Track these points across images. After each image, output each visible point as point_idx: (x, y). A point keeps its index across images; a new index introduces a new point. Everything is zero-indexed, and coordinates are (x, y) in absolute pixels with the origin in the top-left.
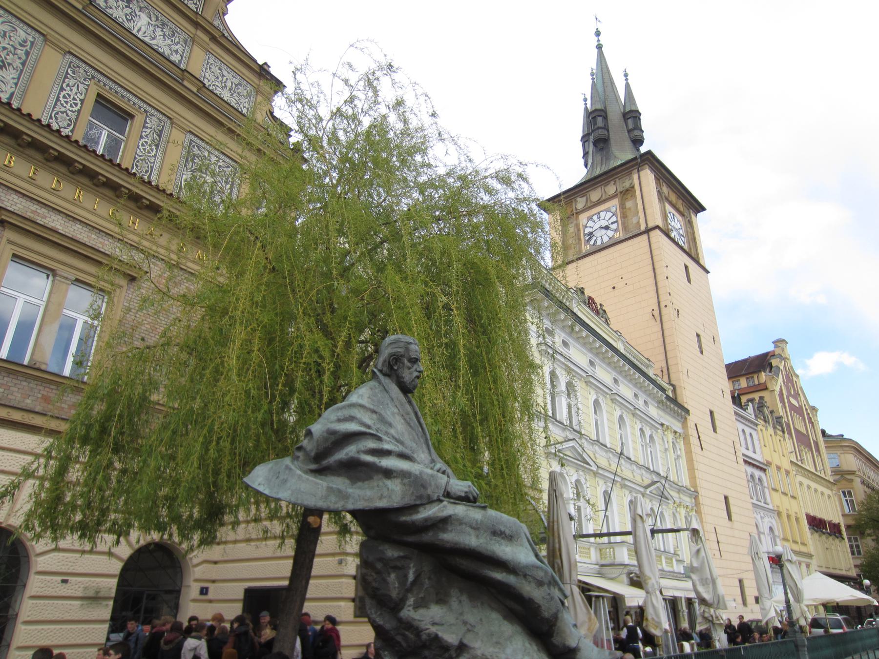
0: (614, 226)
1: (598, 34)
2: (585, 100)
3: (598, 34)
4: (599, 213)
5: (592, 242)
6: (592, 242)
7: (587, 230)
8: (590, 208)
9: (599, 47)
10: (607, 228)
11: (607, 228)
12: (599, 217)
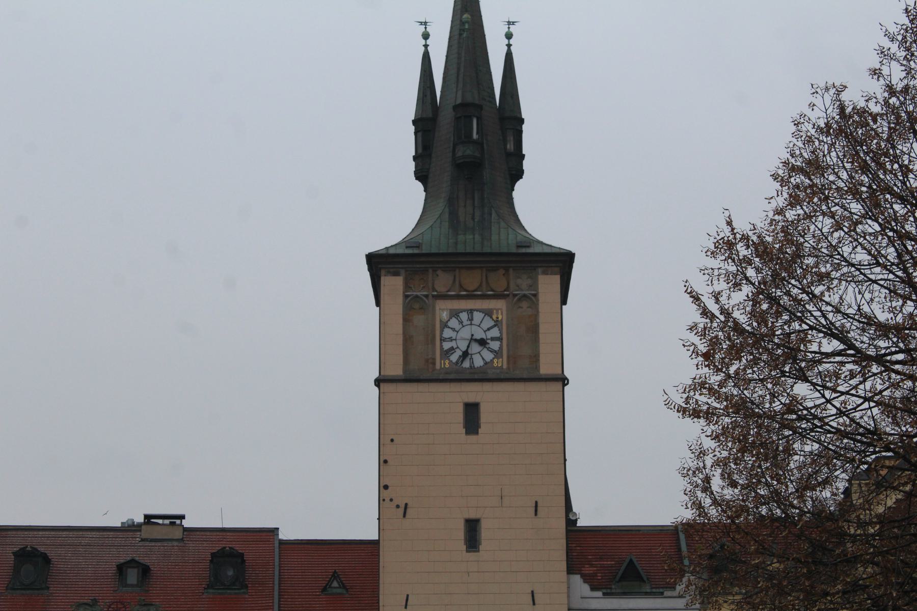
0: (495, 345)
2: (426, 36)
4: (471, 312)
5: (454, 358)
6: (454, 358)
7: (447, 333)
8: (458, 297)
10: (482, 342)
11: (482, 342)
12: (471, 319)
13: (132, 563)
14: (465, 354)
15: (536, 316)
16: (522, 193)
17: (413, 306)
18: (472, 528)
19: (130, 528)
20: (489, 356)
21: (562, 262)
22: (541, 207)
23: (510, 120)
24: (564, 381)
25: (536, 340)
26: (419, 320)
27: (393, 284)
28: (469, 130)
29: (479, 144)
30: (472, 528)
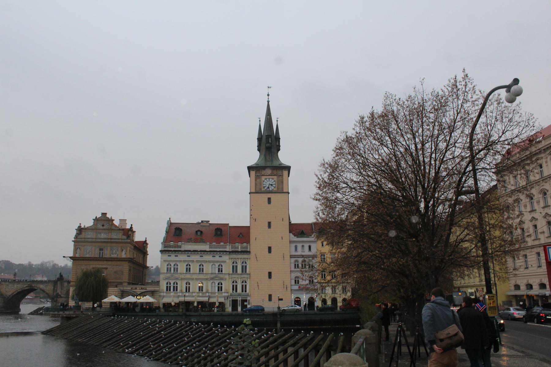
0: (274, 186)
1: (268, 95)
3: (268, 95)
9: (268, 102)
10: (272, 185)
11: (272, 185)
13: (199, 231)
14: (268, 188)
15: (283, 180)
16: (280, 154)
17: (257, 177)
18: (269, 224)
19: (198, 223)
20: (273, 188)
21: (288, 168)
22: (284, 156)
23: (277, 138)
24: (288, 193)
25: (283, 185)
26: (258, 180)
27: (253, 173)
28: (269, 141)
29: (271, 143)
30: (269, 224)
